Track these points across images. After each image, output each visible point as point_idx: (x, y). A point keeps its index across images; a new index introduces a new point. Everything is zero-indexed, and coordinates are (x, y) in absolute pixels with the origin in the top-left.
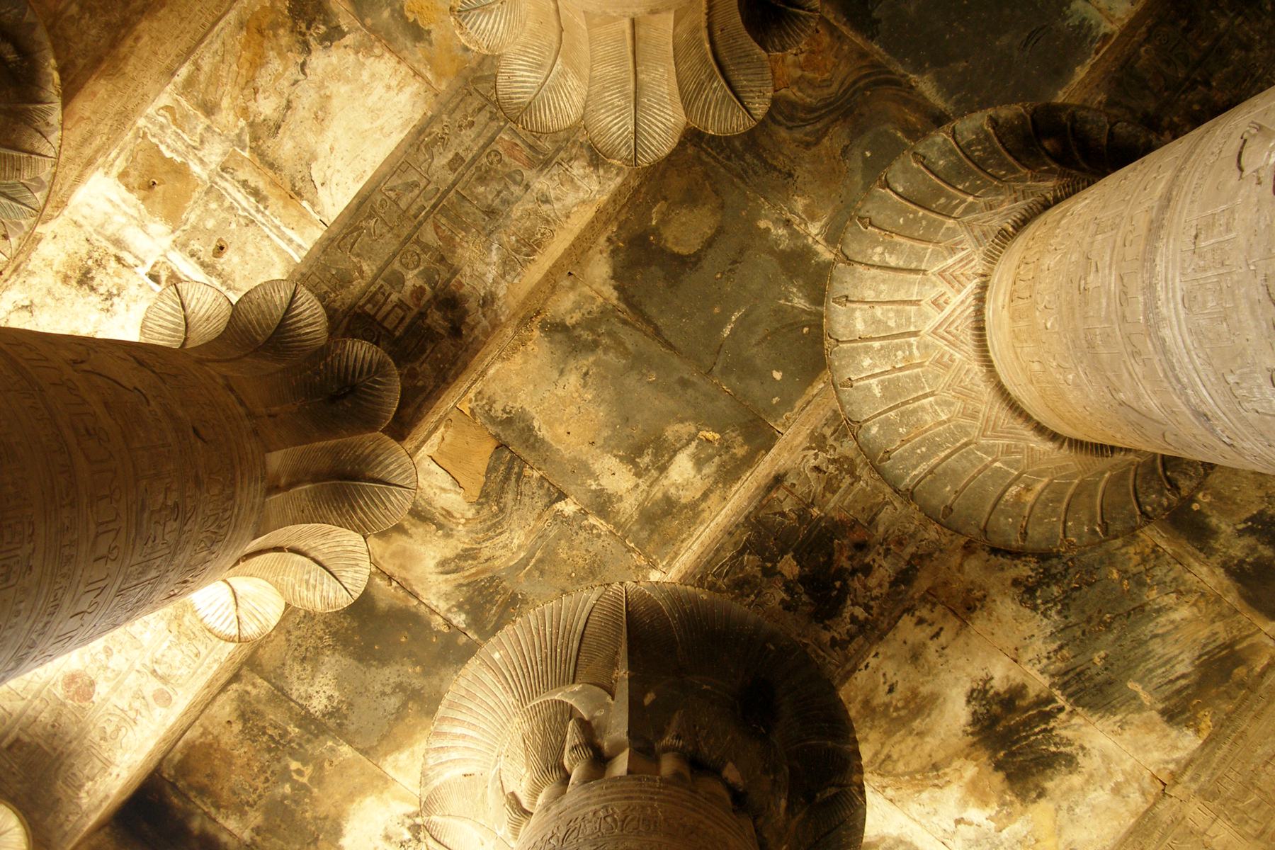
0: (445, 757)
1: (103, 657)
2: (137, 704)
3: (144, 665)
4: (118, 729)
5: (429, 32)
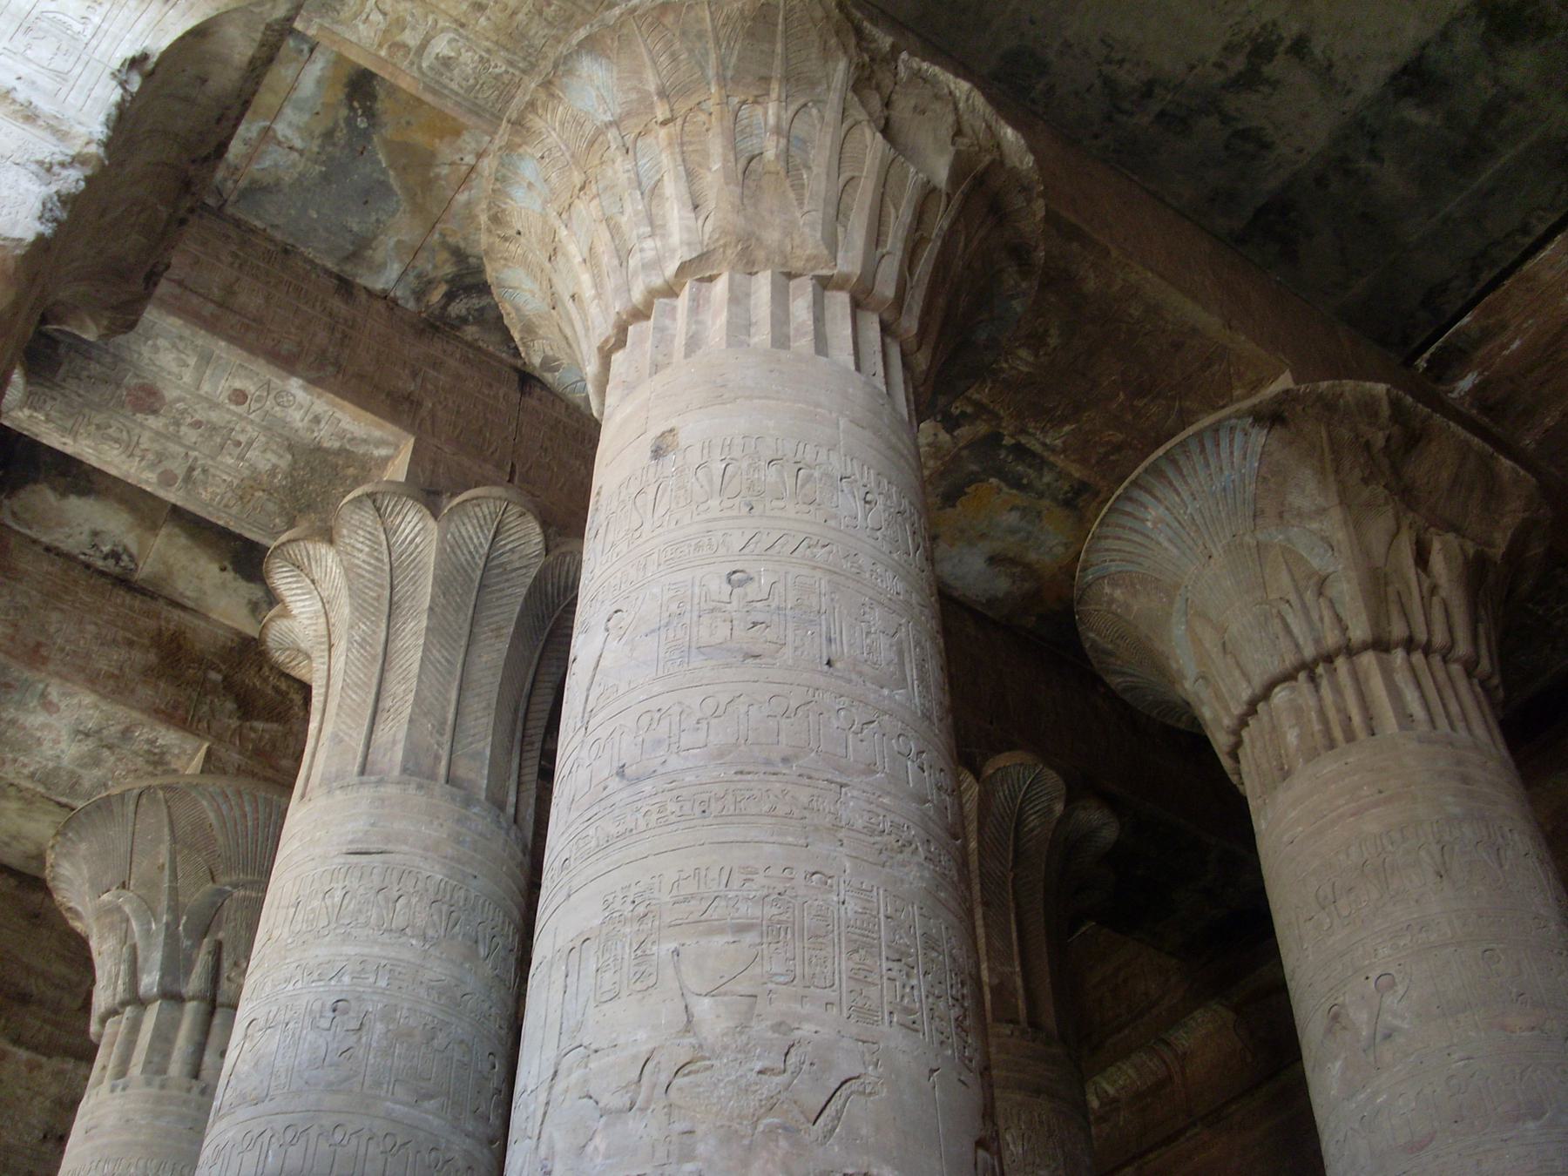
0: (220, 800)
1: (189, 420)
2: (150, 456)
3: (196, 459)
4: (117, 441)
5: (954, 506)
